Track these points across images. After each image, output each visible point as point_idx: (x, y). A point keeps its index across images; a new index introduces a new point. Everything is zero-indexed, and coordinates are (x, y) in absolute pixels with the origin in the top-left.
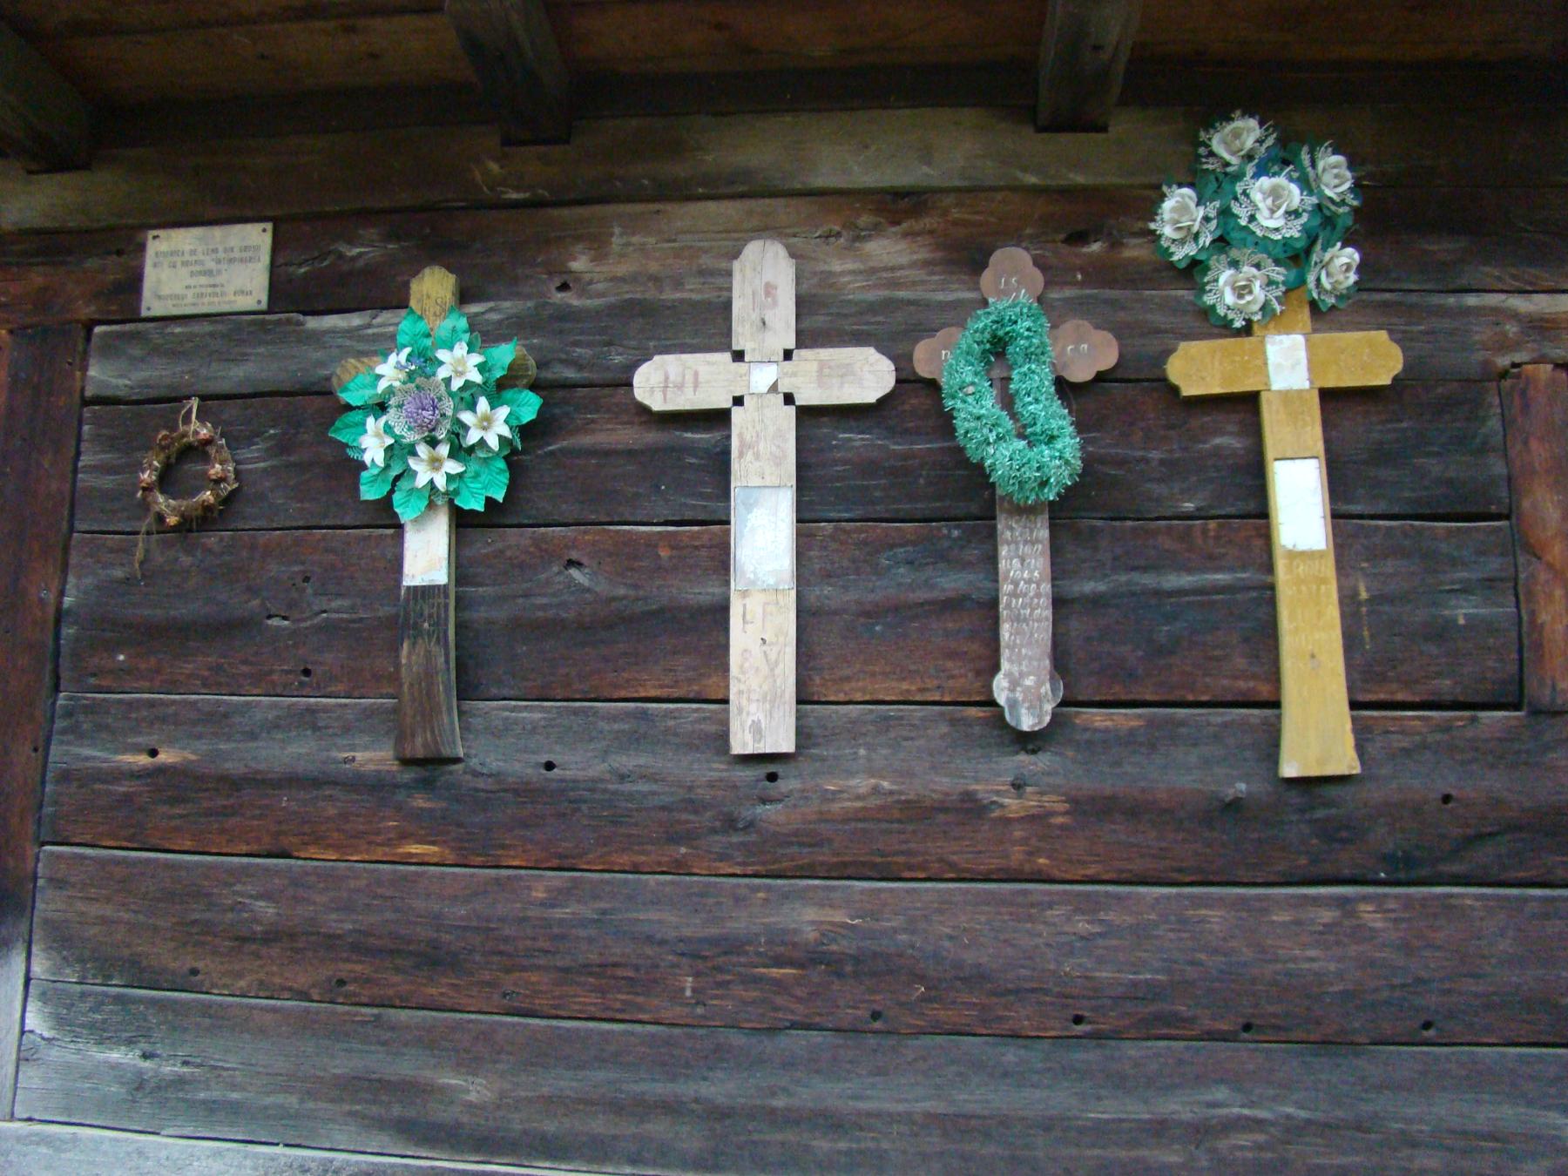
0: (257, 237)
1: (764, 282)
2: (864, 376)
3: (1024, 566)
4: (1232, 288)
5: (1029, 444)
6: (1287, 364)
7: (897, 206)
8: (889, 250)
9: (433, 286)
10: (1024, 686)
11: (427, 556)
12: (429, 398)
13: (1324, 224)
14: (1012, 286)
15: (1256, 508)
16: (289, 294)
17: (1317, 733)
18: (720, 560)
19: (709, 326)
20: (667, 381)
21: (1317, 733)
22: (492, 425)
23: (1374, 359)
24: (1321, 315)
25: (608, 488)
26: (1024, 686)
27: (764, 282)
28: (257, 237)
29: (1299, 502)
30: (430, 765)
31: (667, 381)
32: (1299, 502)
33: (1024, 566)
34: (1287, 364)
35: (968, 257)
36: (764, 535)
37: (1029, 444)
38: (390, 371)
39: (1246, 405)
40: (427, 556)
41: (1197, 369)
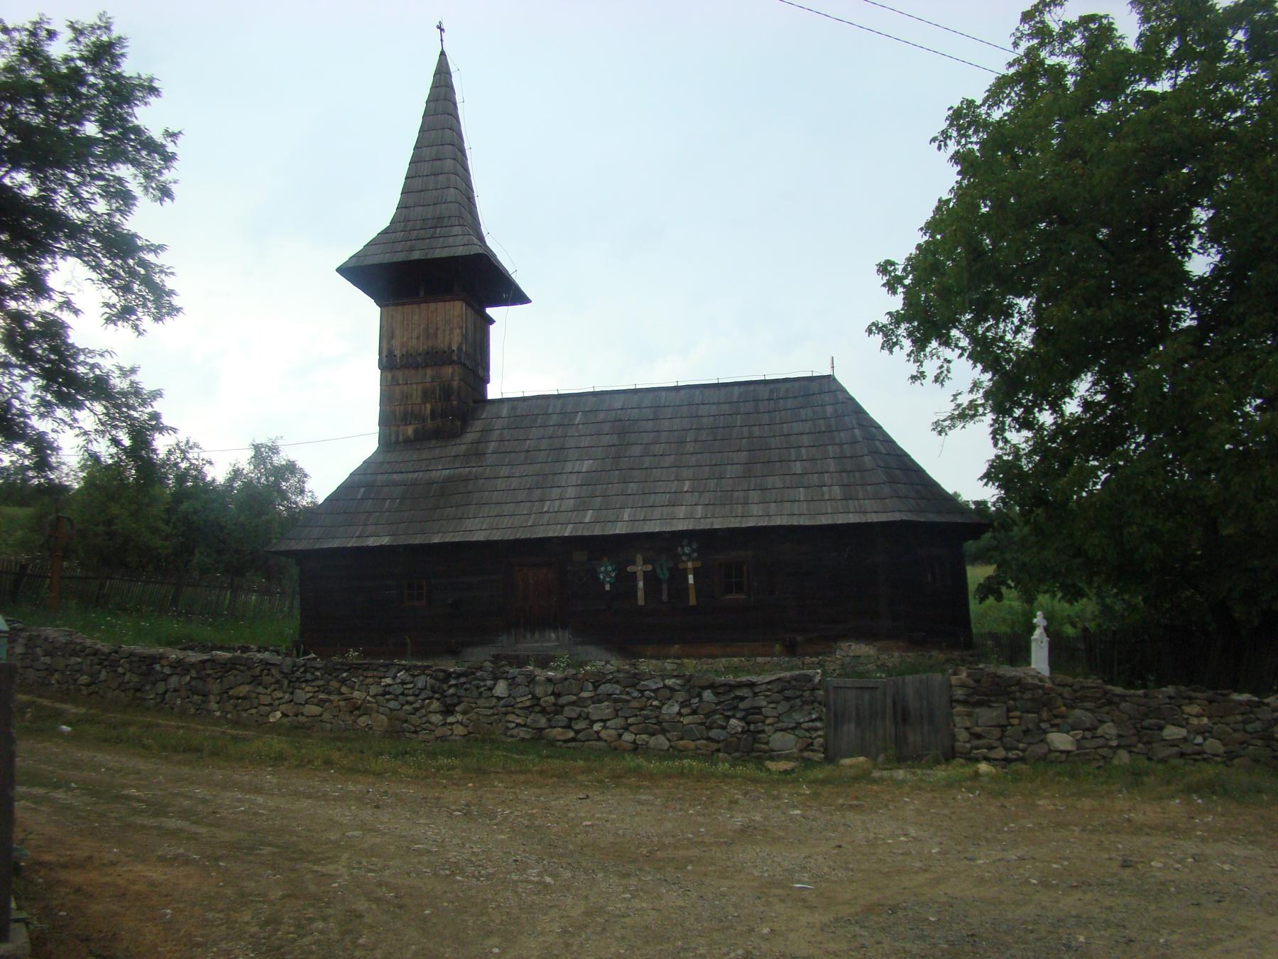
1: (639, 558)
2: (649, 568)
3: (665, 587)
5: (664, 575)
6: (690, 565)
9: (605, 559)
10: (665, 597)
11: (608, 587)
12: (606, 572)
13: (693, 551)
17: (693, 601)
18: (636, 586)
19: (634, 563)
20: (630, 569)
21: (693, 601)
23: (698, 564)
24: (694, 560)
25: (625, 580)
26: (665, 597)
27: (639, 558)
29: (691, 579)
31: (630, 569)
32: (691, 579)
33: (665, 587)
36: (641, 584)
37: (664, 575)
40: (608, 587)
41: (681, 566)
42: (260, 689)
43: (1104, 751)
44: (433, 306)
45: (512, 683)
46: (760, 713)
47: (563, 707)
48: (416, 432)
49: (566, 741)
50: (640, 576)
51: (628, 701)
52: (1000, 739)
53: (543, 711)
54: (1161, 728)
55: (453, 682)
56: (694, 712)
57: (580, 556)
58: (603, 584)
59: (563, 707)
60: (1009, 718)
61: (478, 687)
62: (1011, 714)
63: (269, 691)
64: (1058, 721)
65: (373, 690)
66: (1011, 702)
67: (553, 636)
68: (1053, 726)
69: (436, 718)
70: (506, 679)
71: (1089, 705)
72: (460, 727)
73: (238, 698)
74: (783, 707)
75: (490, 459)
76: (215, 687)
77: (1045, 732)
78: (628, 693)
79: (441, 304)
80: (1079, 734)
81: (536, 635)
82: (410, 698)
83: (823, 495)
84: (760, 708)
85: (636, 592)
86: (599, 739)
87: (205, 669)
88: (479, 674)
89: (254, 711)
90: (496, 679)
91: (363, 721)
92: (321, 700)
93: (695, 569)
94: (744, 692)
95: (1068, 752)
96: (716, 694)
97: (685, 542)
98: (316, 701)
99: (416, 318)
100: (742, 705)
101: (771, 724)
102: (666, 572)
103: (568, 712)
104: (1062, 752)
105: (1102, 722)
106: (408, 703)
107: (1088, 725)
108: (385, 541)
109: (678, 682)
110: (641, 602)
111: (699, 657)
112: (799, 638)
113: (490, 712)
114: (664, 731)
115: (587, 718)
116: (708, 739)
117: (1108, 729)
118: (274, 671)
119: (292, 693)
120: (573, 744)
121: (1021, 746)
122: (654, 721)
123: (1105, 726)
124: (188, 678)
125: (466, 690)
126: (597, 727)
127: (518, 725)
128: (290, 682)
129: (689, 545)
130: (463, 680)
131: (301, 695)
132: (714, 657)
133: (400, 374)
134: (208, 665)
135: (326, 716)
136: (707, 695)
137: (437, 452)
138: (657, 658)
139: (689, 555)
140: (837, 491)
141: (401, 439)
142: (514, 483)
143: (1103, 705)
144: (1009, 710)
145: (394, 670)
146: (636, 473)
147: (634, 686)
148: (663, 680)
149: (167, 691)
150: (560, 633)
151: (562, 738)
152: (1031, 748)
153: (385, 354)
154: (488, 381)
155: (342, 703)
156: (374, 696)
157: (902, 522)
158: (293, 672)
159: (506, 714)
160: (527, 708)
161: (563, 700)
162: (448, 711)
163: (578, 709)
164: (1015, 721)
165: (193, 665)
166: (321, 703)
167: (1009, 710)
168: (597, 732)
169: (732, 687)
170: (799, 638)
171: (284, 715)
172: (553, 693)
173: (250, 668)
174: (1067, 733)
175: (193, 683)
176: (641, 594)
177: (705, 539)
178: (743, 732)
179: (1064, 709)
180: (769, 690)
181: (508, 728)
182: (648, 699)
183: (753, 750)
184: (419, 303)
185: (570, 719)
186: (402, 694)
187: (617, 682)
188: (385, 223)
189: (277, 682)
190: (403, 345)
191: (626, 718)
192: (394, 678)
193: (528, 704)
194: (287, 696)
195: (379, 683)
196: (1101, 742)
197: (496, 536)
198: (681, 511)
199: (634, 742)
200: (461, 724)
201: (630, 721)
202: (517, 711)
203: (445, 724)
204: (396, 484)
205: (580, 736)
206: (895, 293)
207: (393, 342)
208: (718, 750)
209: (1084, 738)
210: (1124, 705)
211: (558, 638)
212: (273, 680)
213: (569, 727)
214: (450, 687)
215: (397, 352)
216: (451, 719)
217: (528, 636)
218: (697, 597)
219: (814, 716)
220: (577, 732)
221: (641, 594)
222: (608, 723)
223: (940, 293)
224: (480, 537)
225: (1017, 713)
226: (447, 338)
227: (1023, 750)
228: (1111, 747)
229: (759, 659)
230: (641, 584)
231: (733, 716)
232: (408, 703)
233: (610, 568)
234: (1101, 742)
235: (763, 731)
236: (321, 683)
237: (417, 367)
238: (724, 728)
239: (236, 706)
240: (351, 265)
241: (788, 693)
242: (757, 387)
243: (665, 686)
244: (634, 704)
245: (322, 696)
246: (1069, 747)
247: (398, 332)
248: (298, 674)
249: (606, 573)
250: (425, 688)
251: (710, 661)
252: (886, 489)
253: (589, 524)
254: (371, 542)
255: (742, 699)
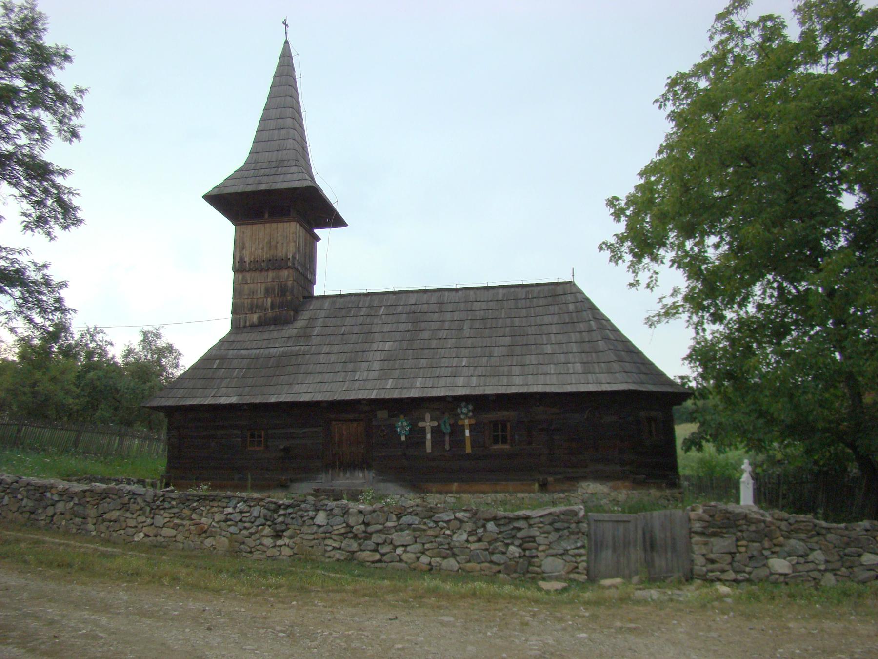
0: (386, 412)
1: (428, 416)
2: (435, 424)
3: (447, 438)
4: (462, 417)
6: (467, 422)
7: (439, 409)
8: (438, 413)
10: (447, 447)
11: (403, 438)
12: (402, 426)
13: (469, 411)
14: (446, 416)
15: (464, 434)
16: (391, 416)
17: (468, 450)
18: (425, 438)
19: (424, 420)
20: (421, 424)
21: (468, 450)
22: (408, 429)
23: (473, 421)
24: (470, 418)
25: (417, 433)
26: (447, 447)
27: (428, 416)
28: (386, 412)
30: (405, 454)
31: (421, 424)
33: (447, 438)
34: (467, 422)
35: (443, 413)
36: (429, 436)
37: (447, 429)
38: (400, 424)
39: (463, 426)
40: (403, 438)
41: (460, 423)
42: (128, 515)
43: (815, 574)
44: (274, 225)
45: (330, 513)
46: (534, 541)
47: (371, 534)
48: (260, 318)
49: (373, 562)
50: (428, 430)
51: (425, 530)
52: (731, 564)
53: (355, 537)
54: (860, 555)
55: (282, 512)
56: (480, 540)
57: (382, 414)
58: (400, 436)
59: (371, 534)
60: (737, 546)
61: (302, 517)
62: (740, 543)
63: (135, 515)
64: (777, 549)
65: (218, 517)
66: (739, 534)
67: (361, 475)
68: (773, 553)
69: (268, 541)
70: (325, 510)
71: (803, 536)
72: (287, 549)
73: (111, 521)
74: (553, 536)
75: (315, 340)
76: (92, 512)
77: (767, 558)
78: (425, 524)
79: (280, 225)
80: (794, 559)
81: (348, 474)
82: (247, 525)
83: (568, 370)
84: (534, 537)
85: (425, 443)
86: (401, 561)
87: (85, 497)
88: (303, 506)
89: (122, 532)
90: (317, 510)
91: (209, 542)
92: (176, 524)
93: (470, 425)
94: (521, 524)
95: (786, 575)
96: (498, 525)
97: (463, 404)
98: (171, 524)
99: (262, 233)
100: (519, 535)
101: (543, 551)
102: (448, 427)
103: (376, 538)
104: (781, 574)
105: (812, 550)
106: (245, 528)
107: (801, 553)
108: (233, 400)
109: (467, 515)
110: (429, 449)
111: (474, 493)
112: (550, 479)
113: (312, 537)
114: (454, 555)
115: (391, 543)
116: (491, 562)
117: (818, 556)
118: (139, 500)
119: (153, 518)
120: (379, 565)
121: (748, 569)
122: (446, 546)
123: (815, 553)
124: (72, 504)
125: (293, 518)
126: (399, 551)
127: (334, 548)
128: (152, 509)
129: (466, 407)
130: (290, 510)
131: (160, 520)
132: (484, 493)
133: (248, 276)
134: (88, 494)
135: (180, 538)
136: (491, 526)
137: (275, 334)
138: (441, 493)
139: (466, 415)
140: (579, 367)
141: (248, 324)
142: (333, 358)
143: (812, 536)
144: (737, 540)
145: (234, 501)
146: (426, 351)
147: (430, 517)
148: (454, 513)
149: (55, 514)
150: (366, 472)
151: (371, 559)
152: (755, 572)
153: (237, 260)
154: (314, 283)
155: (192, 528)
156: (218, 522)
157: (629, 390)
158: (154, 502)
159: (325, 539)
160: (342, 534)
161: (371, 529)
162: (278, 535)
163: (384, 536)
164: (743, 549)
165: (76, 493)
166: (176, 527)
167: (737, 540)
168: (399, 556)
169: (511, 520)
170: (550, 479)
171: (146, 536)
172: (364, 523)
173: (120, 497)
174: (785, 558)
175: (76, 508)
176: (428, 444)
177: (479, 402)
178: (520, 557)
179: (781, 539)
180: (542, 522)
181: (326, 551)
182: (442, 529)
183: (528, 572)
184: (266, 222)
185: (378, 544)
186: (241, 521)
187: (416, 514)
188: (240, 164)
189: (141, 509)
190: (251, 253)
191: (424, 544)
192: (235, 508)
193: (343, 531)
194: (149, 521)
195: (222, 512)
196: (811, 566)
197: (319, 398)
198: (460, 381)
199: (430, 564)
200: (288, 546)
201: (426, 546)
202: (333, 537)
203: (274, 547)
204: (243, 358)
205: (385, 558)
206: (619, 221)
207: (244, 252)
208: (499, 572)
209: (798, 563)
210: (829, 536)
211: (364, 477)
212: (138, 507)
213: (376, 550)
214: (279, 516)
215: (247, 259)
216: (279, 542)
217: (342, 474)
218: (472, 447)
219: (579, 545)
220: (383, 555)
221: (428, 444)
222: (409, 548)
223: (651, 221)
224: (306, 398)
225: (744, 543)
226: (284, 251)
227: (750, 573)
228: (820, 570)
229: (519, 495)
230: (429, 436)
231: (512, 544)
232: (245, 528)
233: (405, 424)
234: (811, 566)
235: (537, 556)
236: (176, 510)
237: (261, 271)
238: (504, 553)
239: (108, 527)
240: (213, 194)
241: (558, 525)
242: (516, 289)
243: (456, 518)
244: (430, 532)
245: (176, 521)
246: (787, 570)
247: (247, 245)
248: (158, 503)
249: (402, 426)
250: (259, 517)
251: (482, 495)
252: (616, 366)
253: (390, 390)
254: (223, 401)
255: (519, 529)
